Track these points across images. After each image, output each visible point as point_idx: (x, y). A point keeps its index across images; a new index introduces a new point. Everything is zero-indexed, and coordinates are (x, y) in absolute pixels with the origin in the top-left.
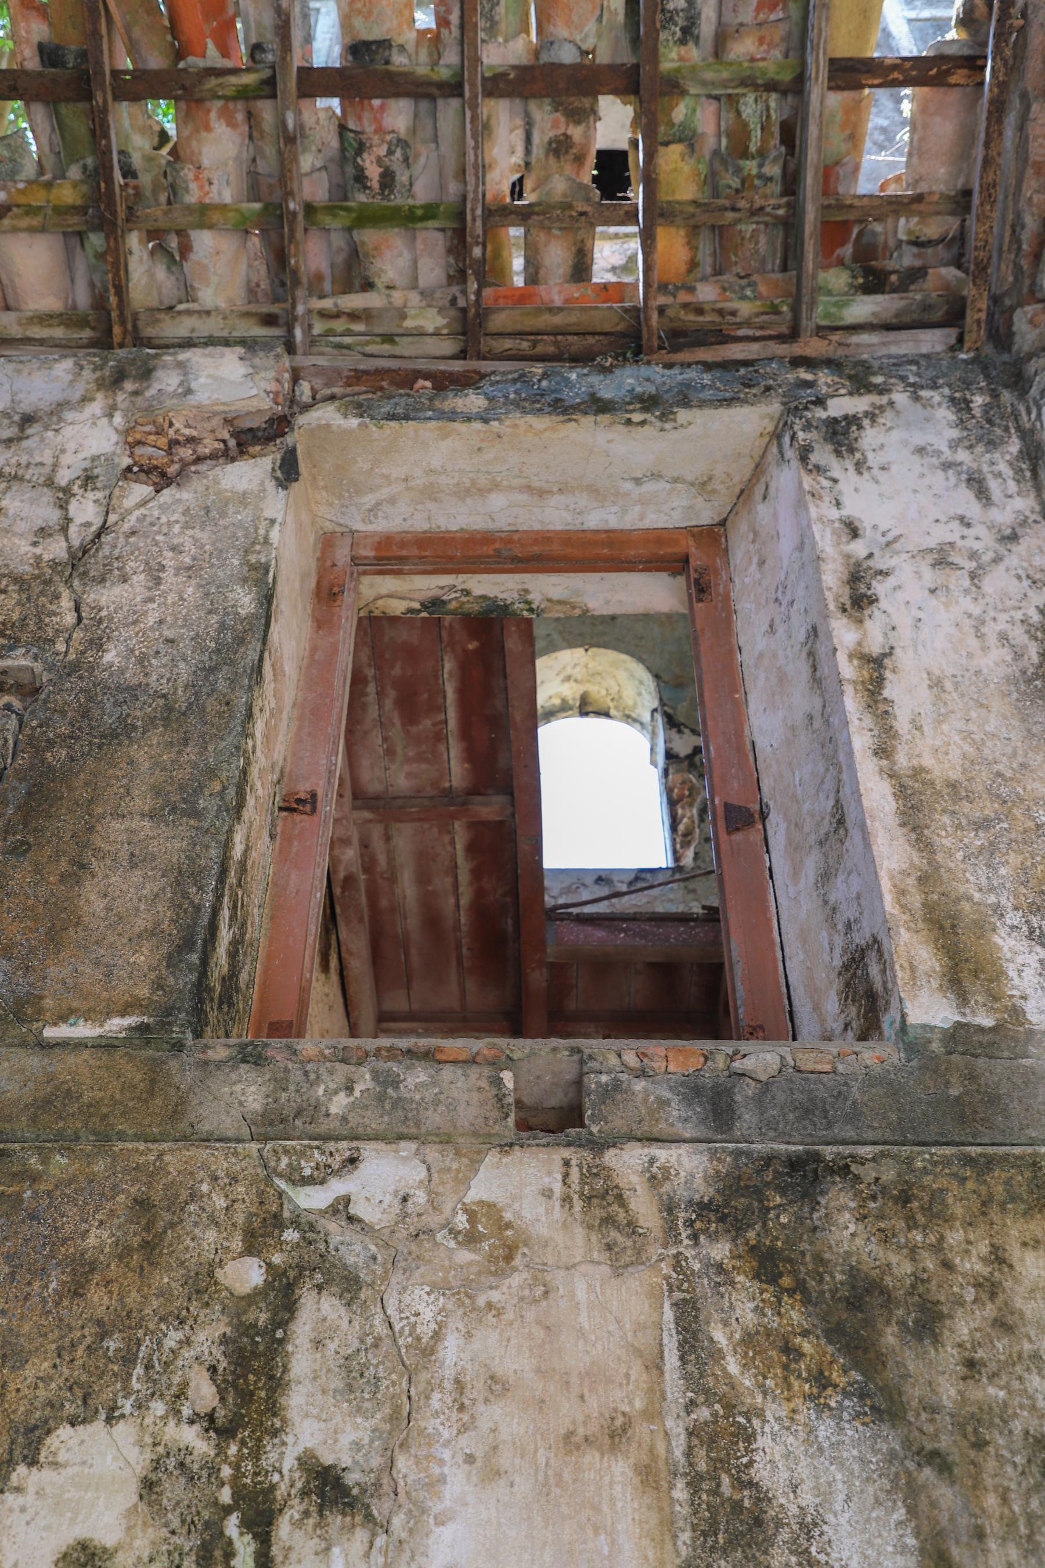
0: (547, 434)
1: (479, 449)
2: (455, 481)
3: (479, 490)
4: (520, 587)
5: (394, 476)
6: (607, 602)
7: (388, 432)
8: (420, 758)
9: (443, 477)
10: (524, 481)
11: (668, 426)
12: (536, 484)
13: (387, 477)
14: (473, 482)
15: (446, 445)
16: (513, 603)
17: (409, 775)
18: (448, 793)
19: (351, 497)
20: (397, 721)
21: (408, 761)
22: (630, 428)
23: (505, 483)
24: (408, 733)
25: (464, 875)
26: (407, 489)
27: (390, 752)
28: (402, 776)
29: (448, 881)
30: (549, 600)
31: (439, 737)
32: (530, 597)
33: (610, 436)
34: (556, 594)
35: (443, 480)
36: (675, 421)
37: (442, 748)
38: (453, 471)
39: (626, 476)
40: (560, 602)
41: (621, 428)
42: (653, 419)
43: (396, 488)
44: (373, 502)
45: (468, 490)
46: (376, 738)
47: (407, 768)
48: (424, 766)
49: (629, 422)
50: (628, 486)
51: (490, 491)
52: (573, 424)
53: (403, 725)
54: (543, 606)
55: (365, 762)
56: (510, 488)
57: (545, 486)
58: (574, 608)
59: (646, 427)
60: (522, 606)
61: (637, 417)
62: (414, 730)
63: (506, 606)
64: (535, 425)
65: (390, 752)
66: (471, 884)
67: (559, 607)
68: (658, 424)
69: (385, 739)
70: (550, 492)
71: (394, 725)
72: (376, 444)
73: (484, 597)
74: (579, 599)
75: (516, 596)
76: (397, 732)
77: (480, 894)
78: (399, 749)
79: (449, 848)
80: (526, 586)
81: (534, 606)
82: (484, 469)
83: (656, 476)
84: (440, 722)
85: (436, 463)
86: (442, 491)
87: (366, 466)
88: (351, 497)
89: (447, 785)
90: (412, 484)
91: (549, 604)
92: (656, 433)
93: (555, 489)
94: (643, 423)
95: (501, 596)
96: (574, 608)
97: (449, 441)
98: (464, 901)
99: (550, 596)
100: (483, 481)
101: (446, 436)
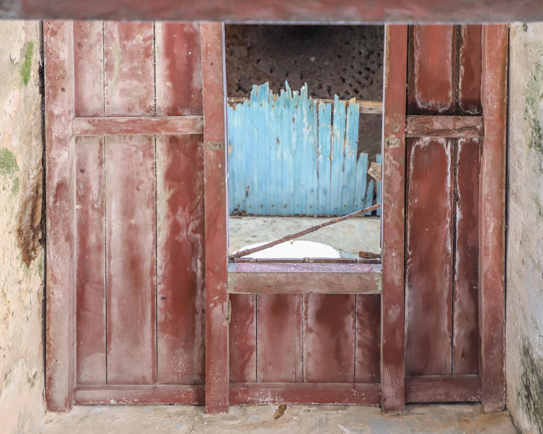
8: (132, 74)
17: (124, 92)
18: (152, 111)
20: (116, 35)
21: (123, 76)
24: (124, 47)
25: (162, 208)
27: (109, 67)
28: (117, 93)
29: (149, 212)
31: (148, 53)
37: (150, 63)
46: (98, 54)
47: (121, 84)
48: (135, 83)
53: (121, 39)
55: (89, 77)
62: (129, 44)
65: (109, 67)
66: (168, 217)
69: (106, 53)
71: (114, 39)
76: (115, 47)
77: (175, 229)
78: (116, 64)
79: (151, 175)
84: (149, 38)
89: (152, 103)
98: (162, 238)
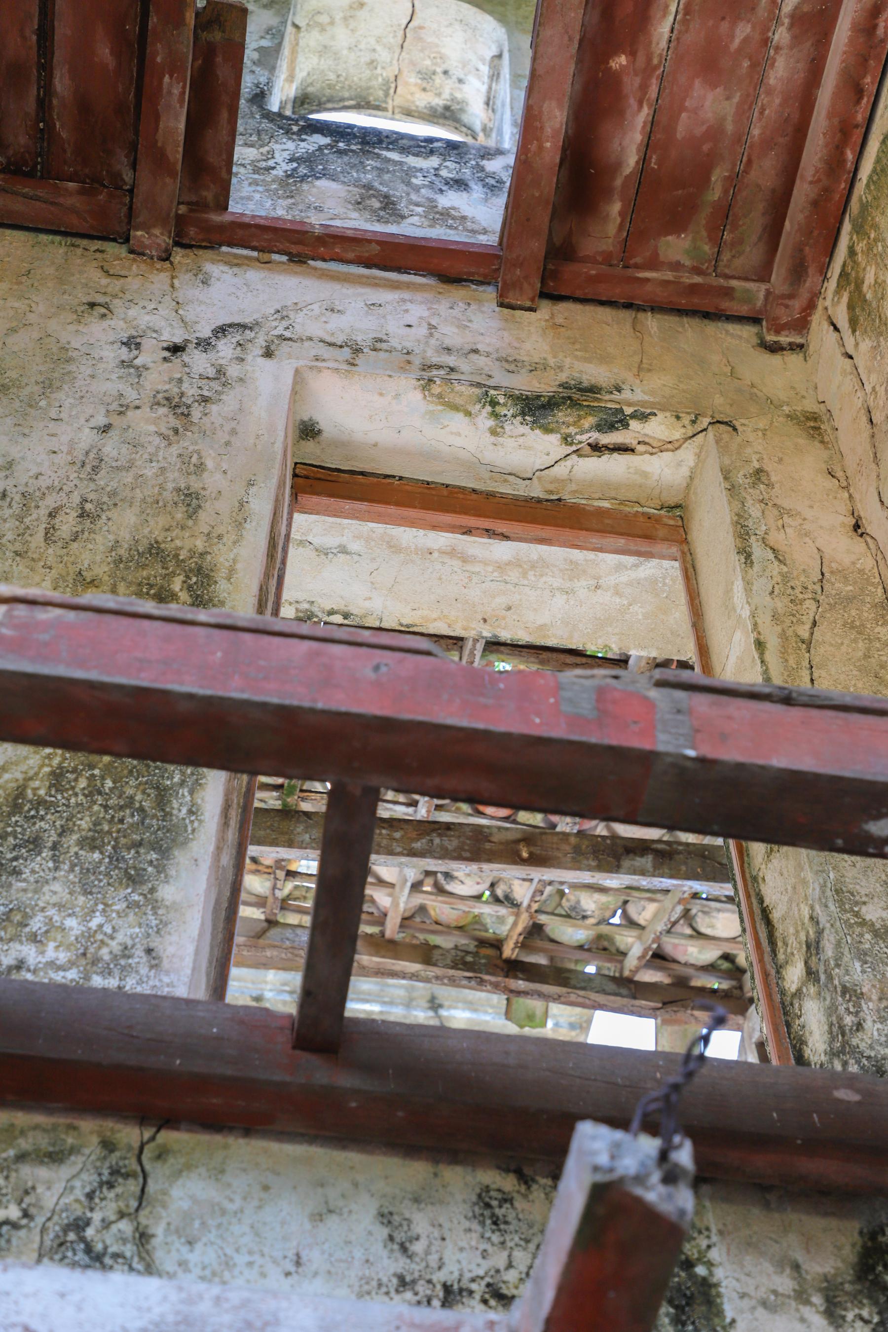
0: (435, 615)
1: (509, 608)
2: (544, 579)
3: (520, 566)
4: (501, 439)
5: (609, 593)
6: (397, 396)
7: (600, 641)
9: (555, 585)
10: (469, 567)
11: (306, 606)
12: (456, 563)
13: (617, 593)
14: (524, 575)
15: (543, 618)
16: (514, 416)
19: (664, 578)
22: (346, 609)
23: (490, 569)
26: (598, 578)
30: (468, 414)
32: (491, 423)
33: (367, 604)
34: (458, 421)
35: (557, 582)
36: (297, 609)
38: (543, 589)
39: (356, 557)
40: (455, 408)
41: (355, 611)
42: (320, 614)
43: (612, 580)
44: (641, 568)
45: (533, 567)
49: (346, 616)
50: (354, 546)
51: (509, 563)
52: (405, 622)
54: (478, 406)
56: (485, 563)
57: (446, 559)
58: (440, 396)
59: (328, 607)
60: (502, 411)
61: (338, 619)
63: (523, 414)
64: (446, 626)
67: (459, 401)
68: (315, 609)
70: (442, 552)
72: (617, 630)
73: (547, 430)
74: (432, 407)
75: (508, 427)
80: (493, 439)
81: (488, 408)
82: (509, 586)
83: (323, 552)
85: (560, 600)
86: (561, 570)
87: (635, 608)
88: (664, 578)
90: (593, 582)
91: (470, 408)
92: (320, 601)
93: (436, 555)
94: (331, 613)
95: (526, 429)
96: (440, 396)
97: (540, 622)
99: (467, 419)
100: (513, 575)
101: (542, 627)
